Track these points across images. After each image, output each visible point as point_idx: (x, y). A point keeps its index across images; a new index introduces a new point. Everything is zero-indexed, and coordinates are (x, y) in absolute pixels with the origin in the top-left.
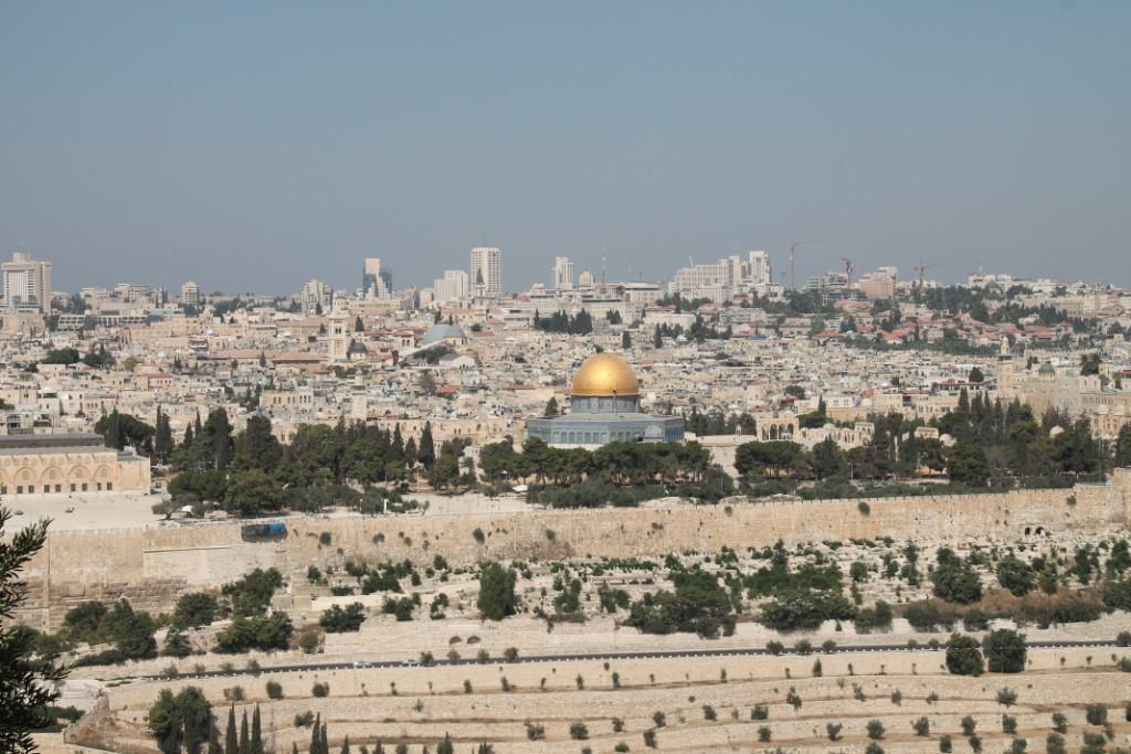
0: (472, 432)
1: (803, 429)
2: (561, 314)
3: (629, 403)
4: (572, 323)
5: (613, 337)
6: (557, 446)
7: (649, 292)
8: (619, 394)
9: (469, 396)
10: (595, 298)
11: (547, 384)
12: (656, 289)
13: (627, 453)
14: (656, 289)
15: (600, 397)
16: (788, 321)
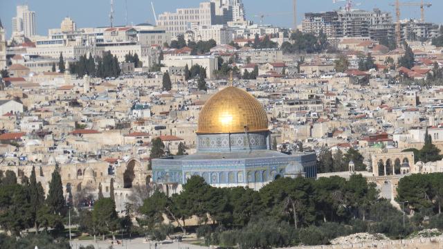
0: (72, 178)
1: (419, 163)
2: (88, 57)
3: (260, 138)
4: (99, 66)
5: (147, 80)
6: (217, 186)
7: (157, 35)
8: (251, 130)
9: (38, 141)
10: (105, 42)
11: (112, 128)
12: (164, 32)
13: (301, 188)
14: (164, 32)
15: (230, 134)
16: (308, 60)
